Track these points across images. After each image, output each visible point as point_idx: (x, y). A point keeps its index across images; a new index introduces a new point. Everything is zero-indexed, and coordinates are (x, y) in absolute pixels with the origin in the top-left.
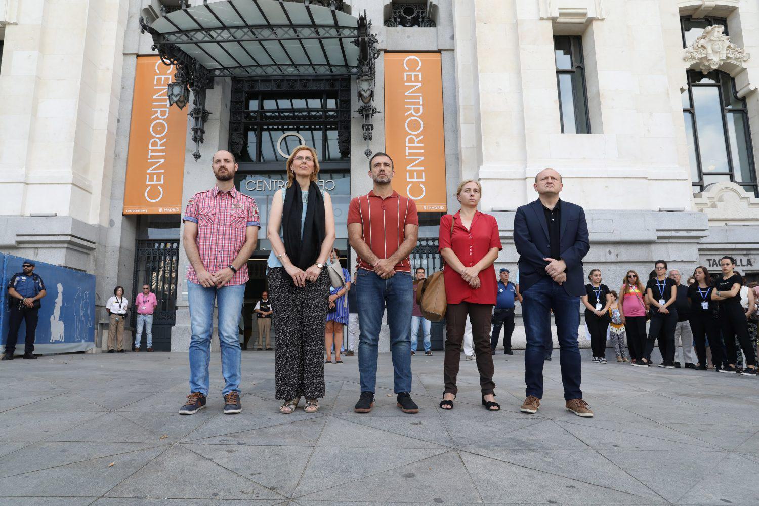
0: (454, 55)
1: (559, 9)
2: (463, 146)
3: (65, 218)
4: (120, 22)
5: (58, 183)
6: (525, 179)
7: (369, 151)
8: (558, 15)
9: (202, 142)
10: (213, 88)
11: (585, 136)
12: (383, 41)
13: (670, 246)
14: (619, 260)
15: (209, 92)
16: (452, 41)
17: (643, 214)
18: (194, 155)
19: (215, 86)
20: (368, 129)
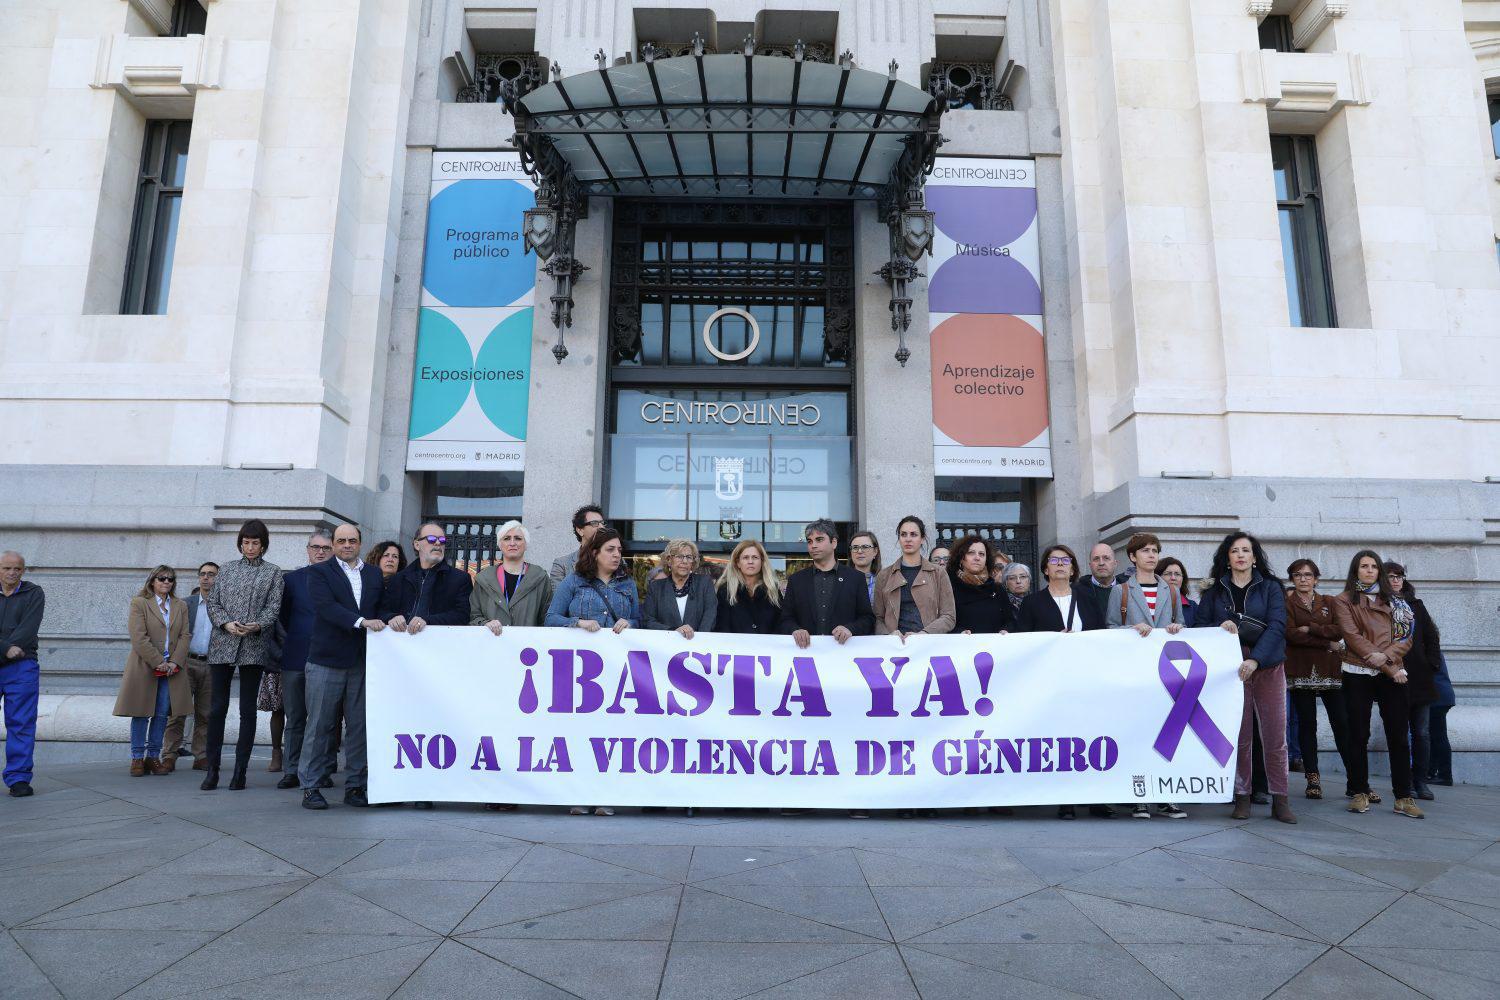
1: (1283, 83)
2: (1089, 345)
3: (310, 475)
4: (404, 85)
5: (295, 404)
7: (904, 352)
8: (1279, 96)
9: (569, 325)
10: (587, 218)
11: (1325, 332)
15: (580, 225)
18: (555, 352)
19: (591, 213)
20: (903, 307)
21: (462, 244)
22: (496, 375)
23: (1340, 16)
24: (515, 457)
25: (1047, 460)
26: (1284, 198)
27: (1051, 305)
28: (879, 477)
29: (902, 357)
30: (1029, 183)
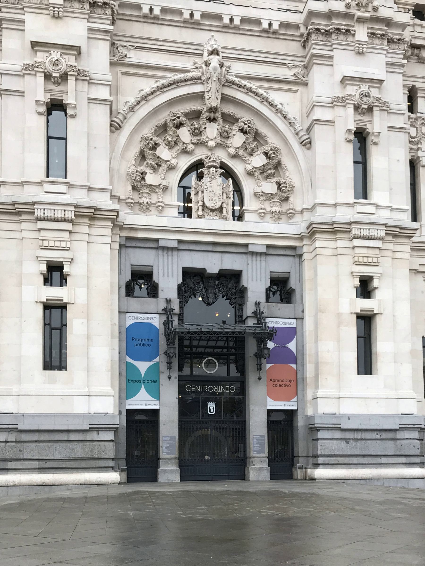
0: (303, 322)
2: (308, 376)
6: (339, 398)
12: (266, 312)
13: (405, 431)
14: (381, 438)
16: (302, 313)
17: (393, 416)
21: (136, 342)
22: (149, 382)
23: (377, 288)
24: (156, 405)
25: (296, 405)
26: (363, 334)
27: (299, 362)
28: (253, 410)
29: (260, 378)
30: (294, 326)
